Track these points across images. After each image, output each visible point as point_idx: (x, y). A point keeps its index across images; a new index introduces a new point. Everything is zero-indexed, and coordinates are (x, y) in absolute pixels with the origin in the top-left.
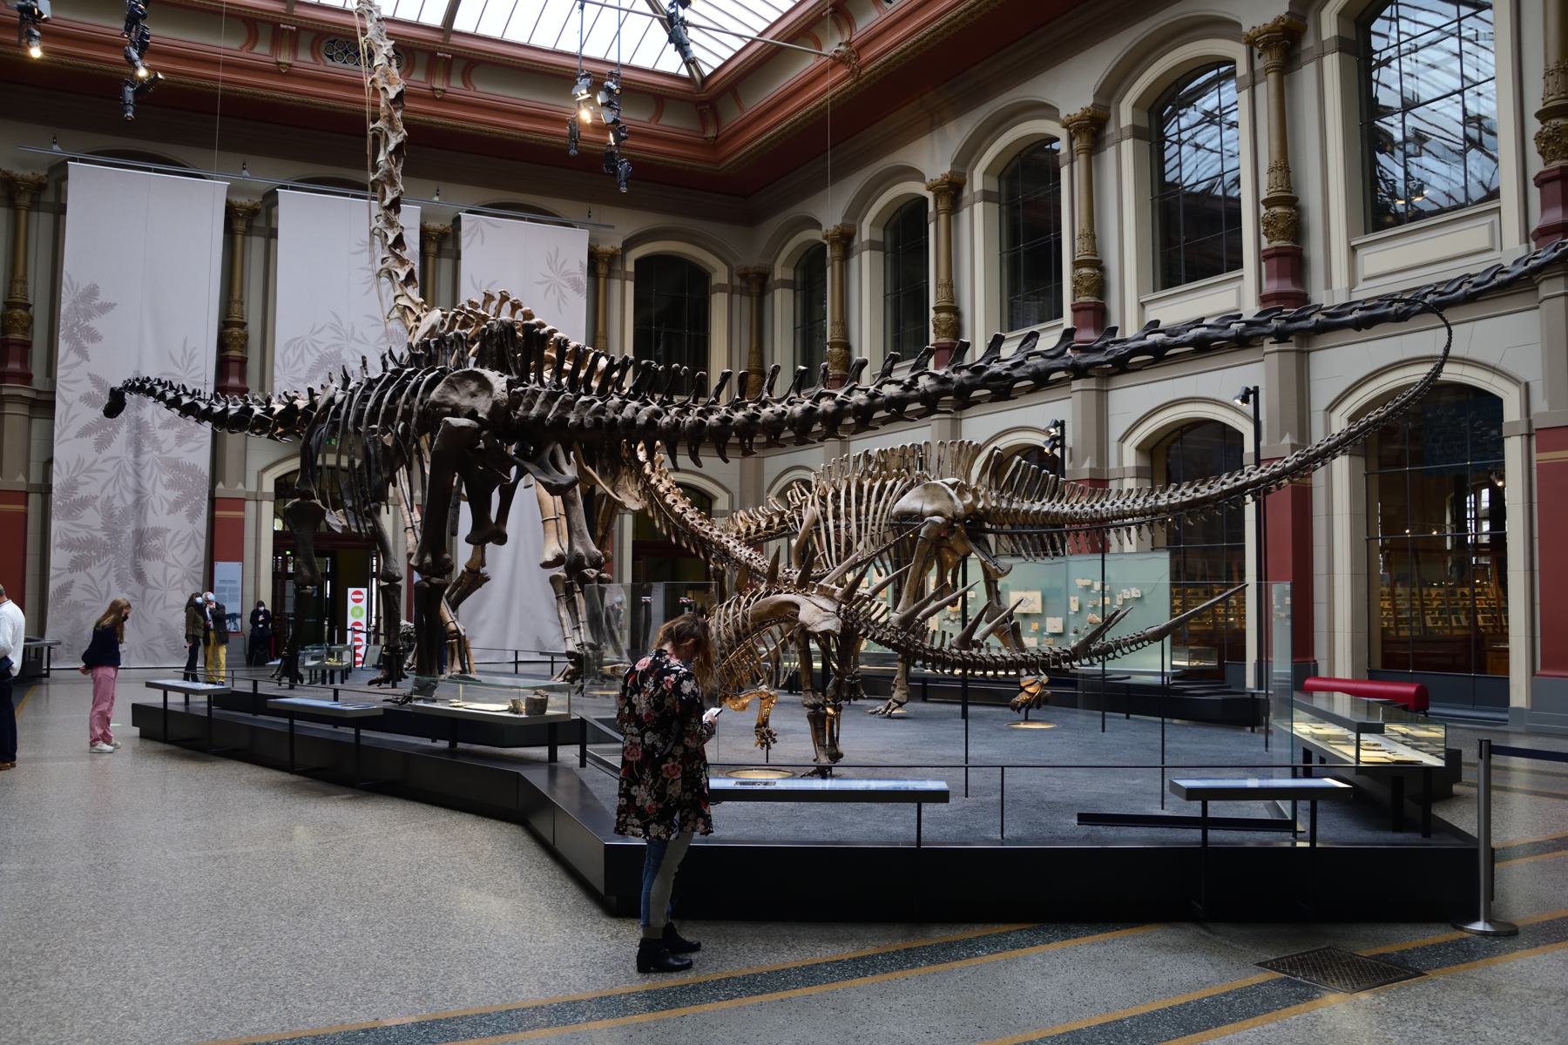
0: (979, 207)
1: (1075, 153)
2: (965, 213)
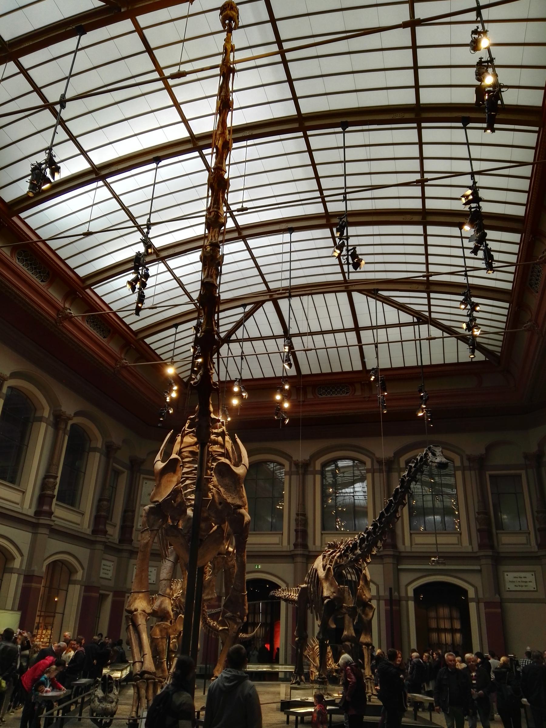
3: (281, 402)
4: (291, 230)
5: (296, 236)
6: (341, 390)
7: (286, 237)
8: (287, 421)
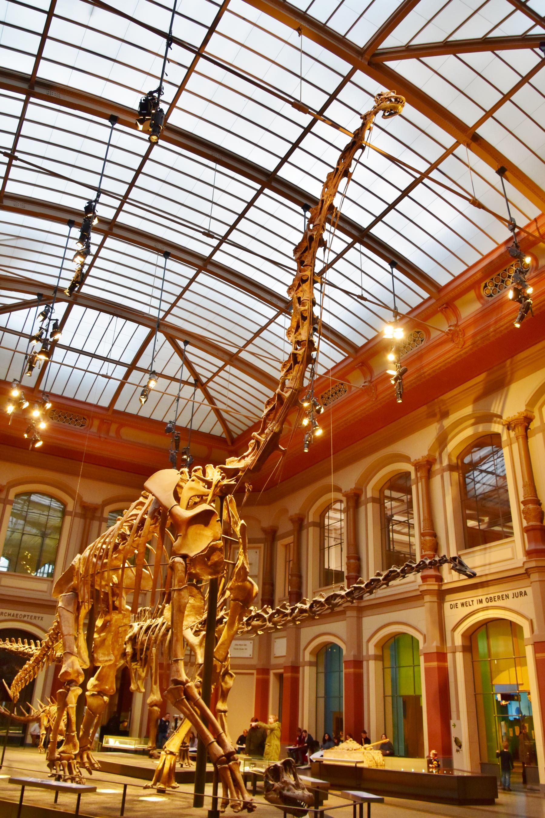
0: (370, 506)
1: (419, 479)
2: (362, 509)
3: (38, 421)
4: (167, 255)
5: (171, 264)
6: (76, 420)
7: (161, 260)
8: (39, 444)
